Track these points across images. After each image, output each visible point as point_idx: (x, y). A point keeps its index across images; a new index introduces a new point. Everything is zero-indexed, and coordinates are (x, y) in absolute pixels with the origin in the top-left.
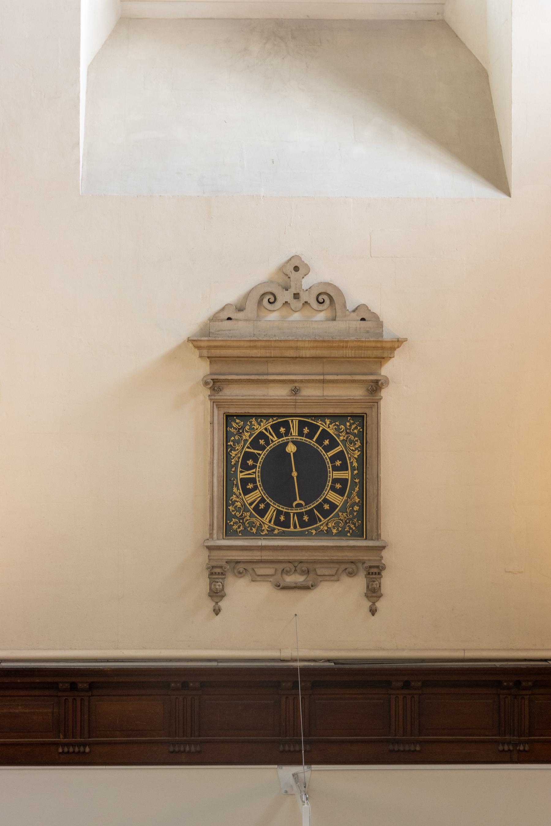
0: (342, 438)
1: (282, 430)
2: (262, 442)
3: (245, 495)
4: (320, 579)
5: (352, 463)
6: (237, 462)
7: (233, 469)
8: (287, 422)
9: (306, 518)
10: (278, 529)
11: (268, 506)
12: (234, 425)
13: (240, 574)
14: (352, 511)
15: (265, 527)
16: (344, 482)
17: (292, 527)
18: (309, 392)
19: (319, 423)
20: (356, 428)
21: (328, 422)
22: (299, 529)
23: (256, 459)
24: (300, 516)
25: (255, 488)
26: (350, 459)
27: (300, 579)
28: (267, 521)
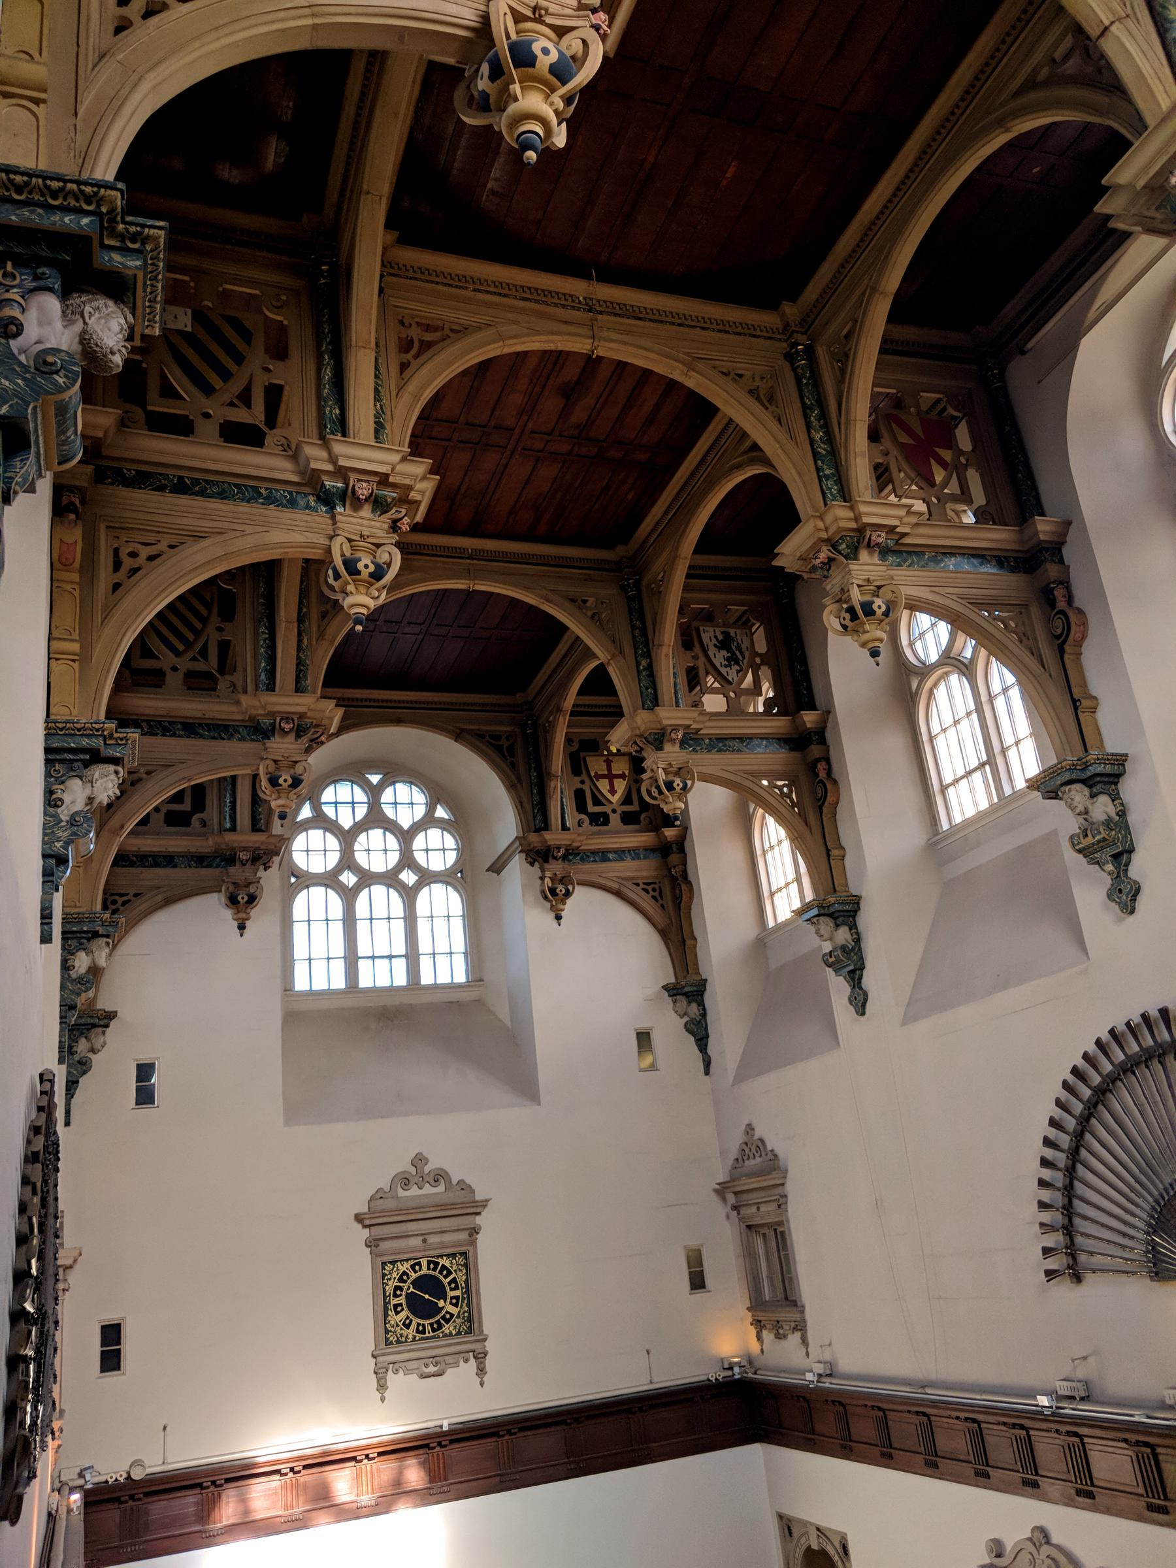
10: (419, 1336)
11: (411, 1321)
13: (396, 1372)
14: (464, 1317)
15: (410, 1336)
16: (457, 1298)
18: (432, 1239)
19: (440, 1260)
22: (432, 1334)
24: (432, 1325)
25: (403, 1309)
27: (432, 1369)
28: (411, 1332)
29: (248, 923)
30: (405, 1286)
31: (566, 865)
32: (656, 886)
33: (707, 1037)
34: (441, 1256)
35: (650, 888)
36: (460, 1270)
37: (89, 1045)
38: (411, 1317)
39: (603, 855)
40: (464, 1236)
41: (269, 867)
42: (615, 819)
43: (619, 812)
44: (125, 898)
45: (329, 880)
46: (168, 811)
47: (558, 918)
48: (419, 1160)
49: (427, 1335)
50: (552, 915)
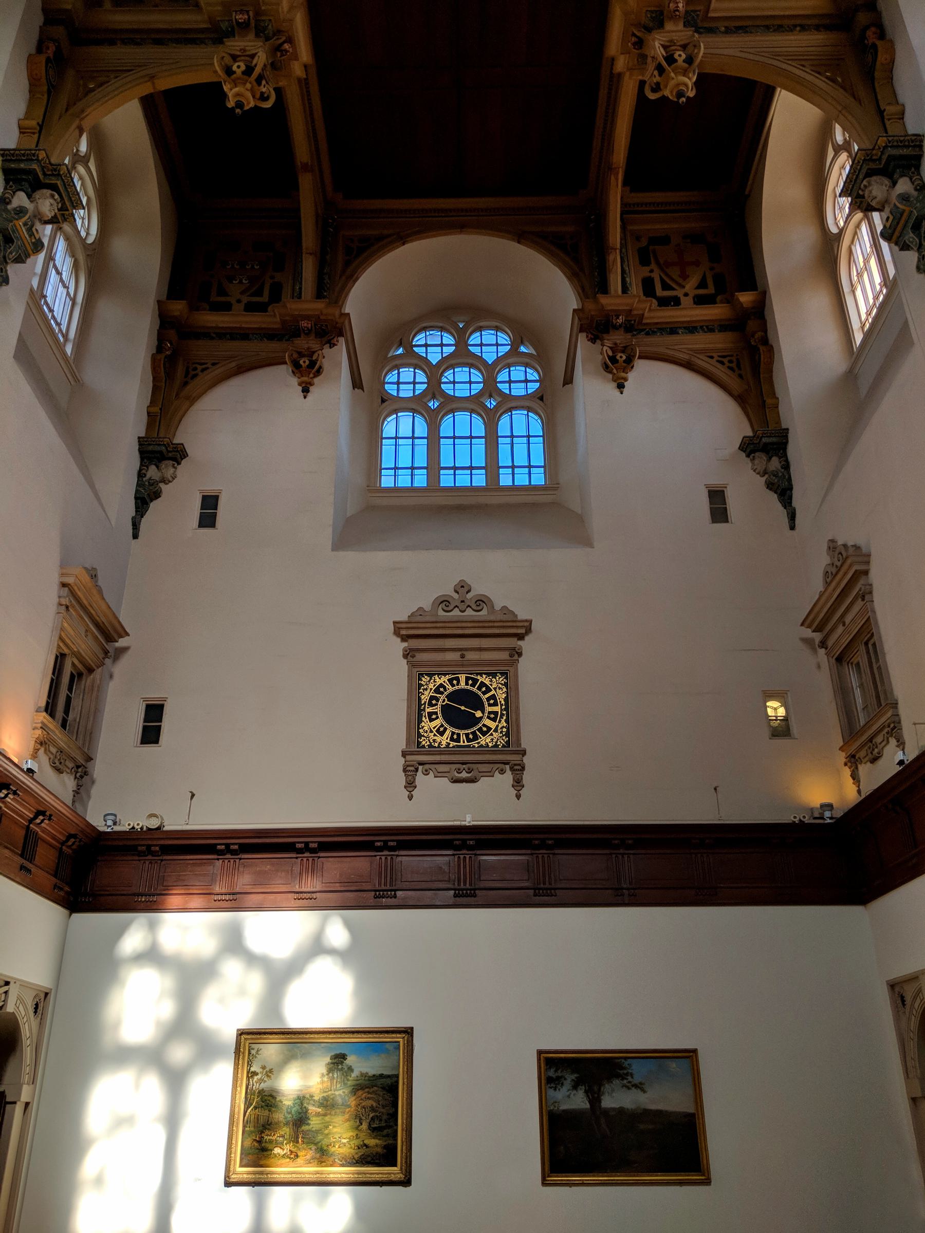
0: (494, 686)
1: (455, 682)
2: (442, 689)
3: (430, 722)
5: (500, 702)
6: (425, 702)
7: (423, 706)
9: (471, 736)
10: (452, 744)
11: (445, 729)
12: (423, 679)
13: (426, 773)
14: (501, 732)
16: (496, 713)
17: (462, 742)
18: (470, 656)
20: (503, 680)
23: (437, 700)
24: (467, 735)
25: (437, 718)
26: (499, 699)
29: (311, 388)
30: (442, 697)
31: (629, 336)
32: (734, 359)
33: (791, 488)
34: (481, 674)
35: (725, 360)
36: (500, 688)
37: (159, 474)
38: (446, 725)
39: (672, 329)
41: (335, 345)
42: (686, 301)
43: (691, 295)
44: (204, 366)
45: (416, 405)
46: (248, 302)
47: (621, 387)
48: (463, 587)
49: (462, 743)
50: (615, 384)
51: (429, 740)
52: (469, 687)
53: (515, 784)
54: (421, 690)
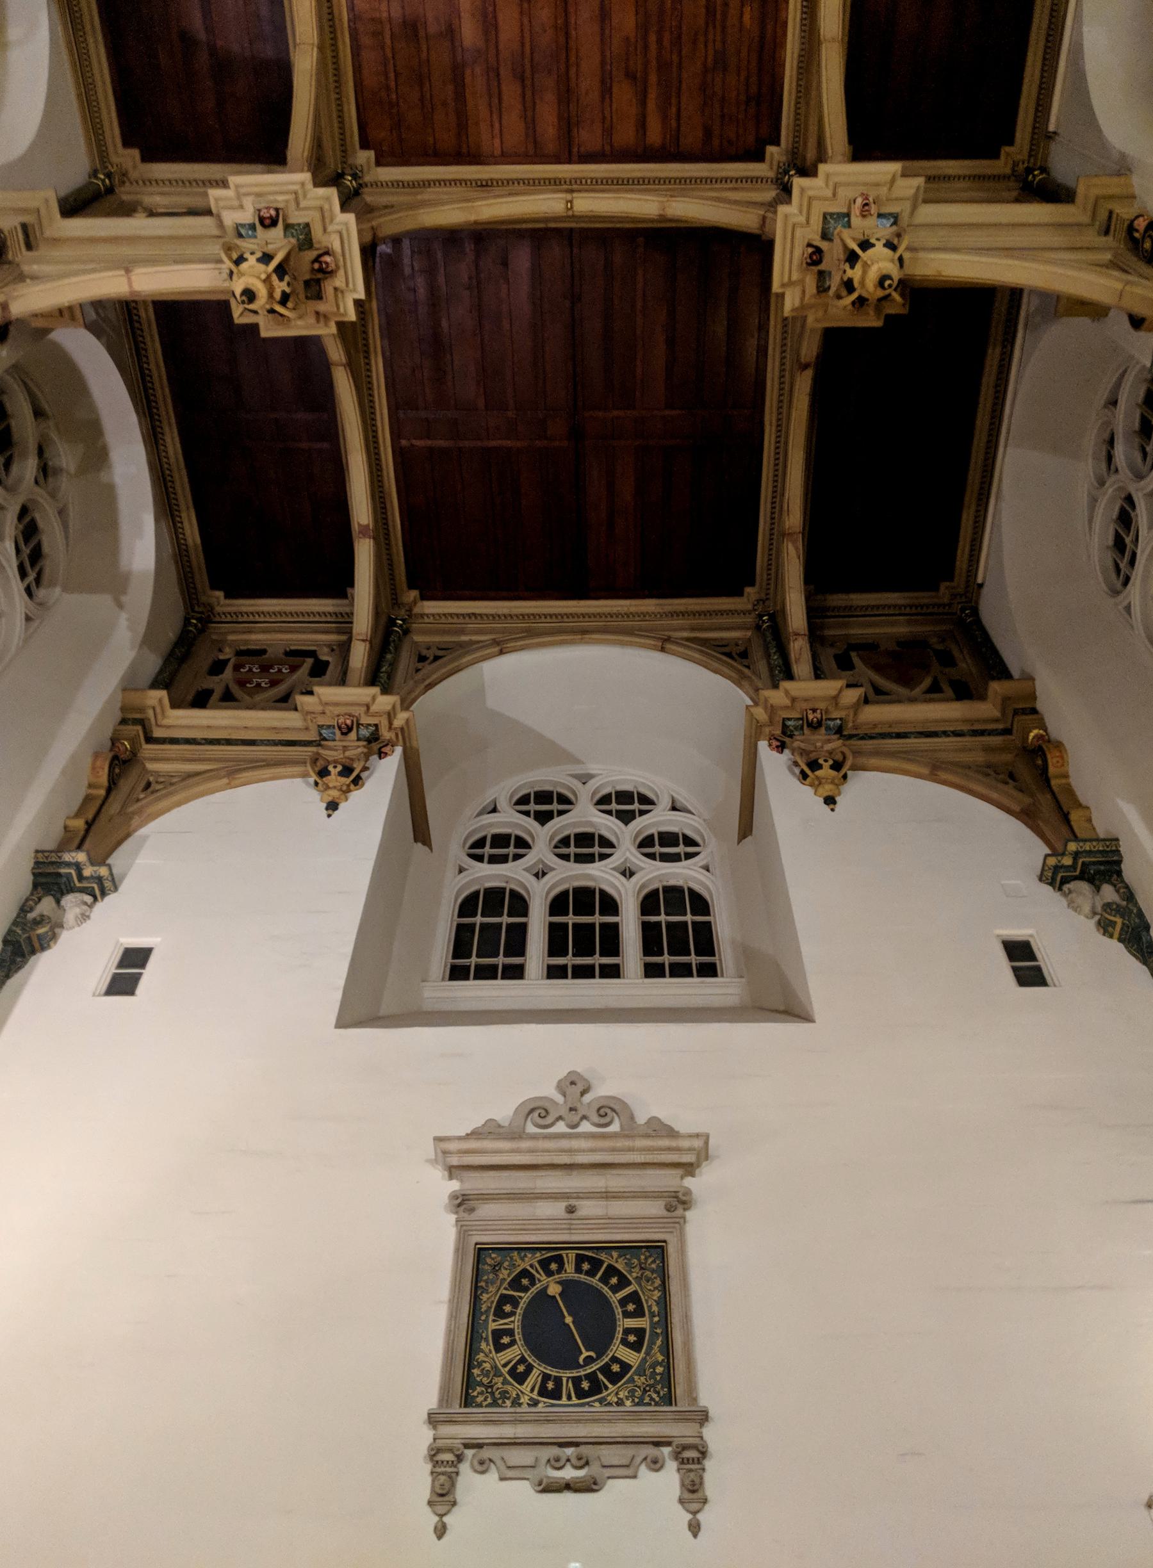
0: (634, 1275)
1: (554, 1266)
2: (525, 1282)
4: (608, 1472)
5: (650, 1307)
7: (483, 1318)
8: (560, 1256)
9: (585, 1385)
11: (529, 1368)
12: (489, 1260)
13: (482, 1467)
16: (640, 1332)
17: (564, 1398)
18: (588, 1208)
19: (603, 1256)
20: (654, 1262)
21: (615, 1254)
22: (575, 1401)
24: (577, 1381)
25: (513, 1343)
26: (647, 1301)
38: (531, 1359)
40: (655, 1208)
51: (492, 1394)
52: (583, 1277)
53: (687, 1495)
54: (483, 1284)
